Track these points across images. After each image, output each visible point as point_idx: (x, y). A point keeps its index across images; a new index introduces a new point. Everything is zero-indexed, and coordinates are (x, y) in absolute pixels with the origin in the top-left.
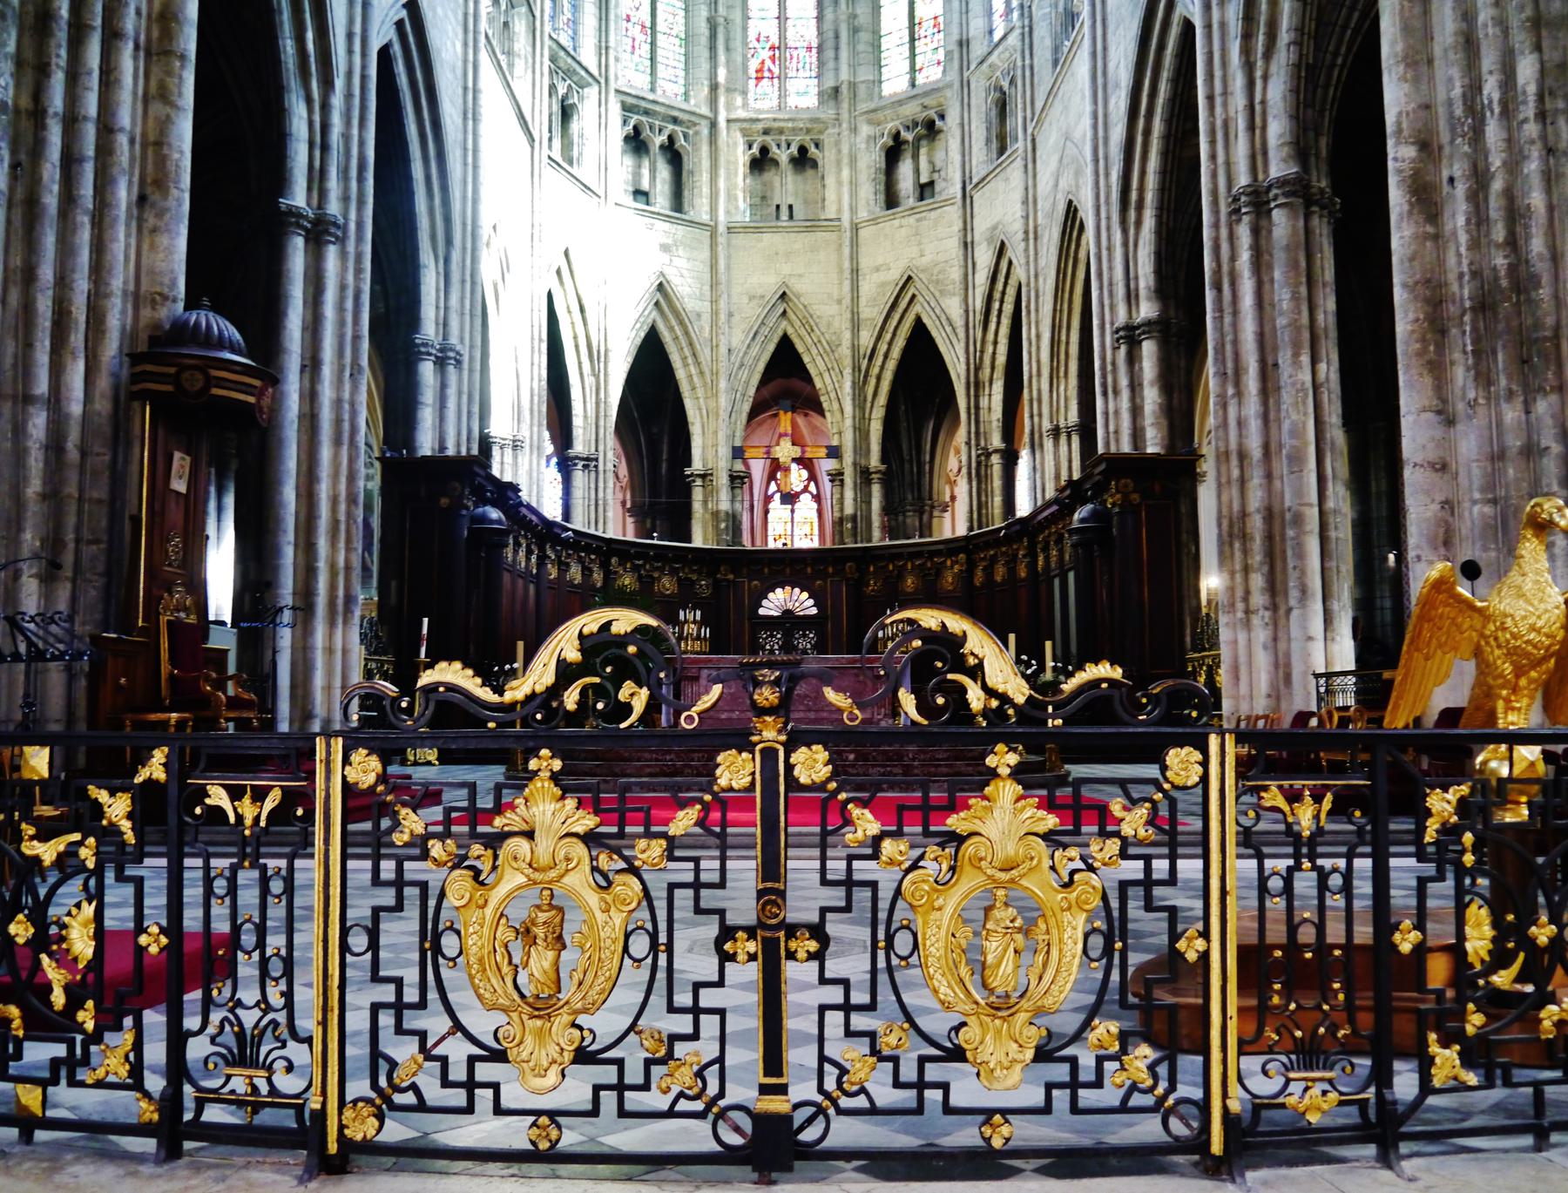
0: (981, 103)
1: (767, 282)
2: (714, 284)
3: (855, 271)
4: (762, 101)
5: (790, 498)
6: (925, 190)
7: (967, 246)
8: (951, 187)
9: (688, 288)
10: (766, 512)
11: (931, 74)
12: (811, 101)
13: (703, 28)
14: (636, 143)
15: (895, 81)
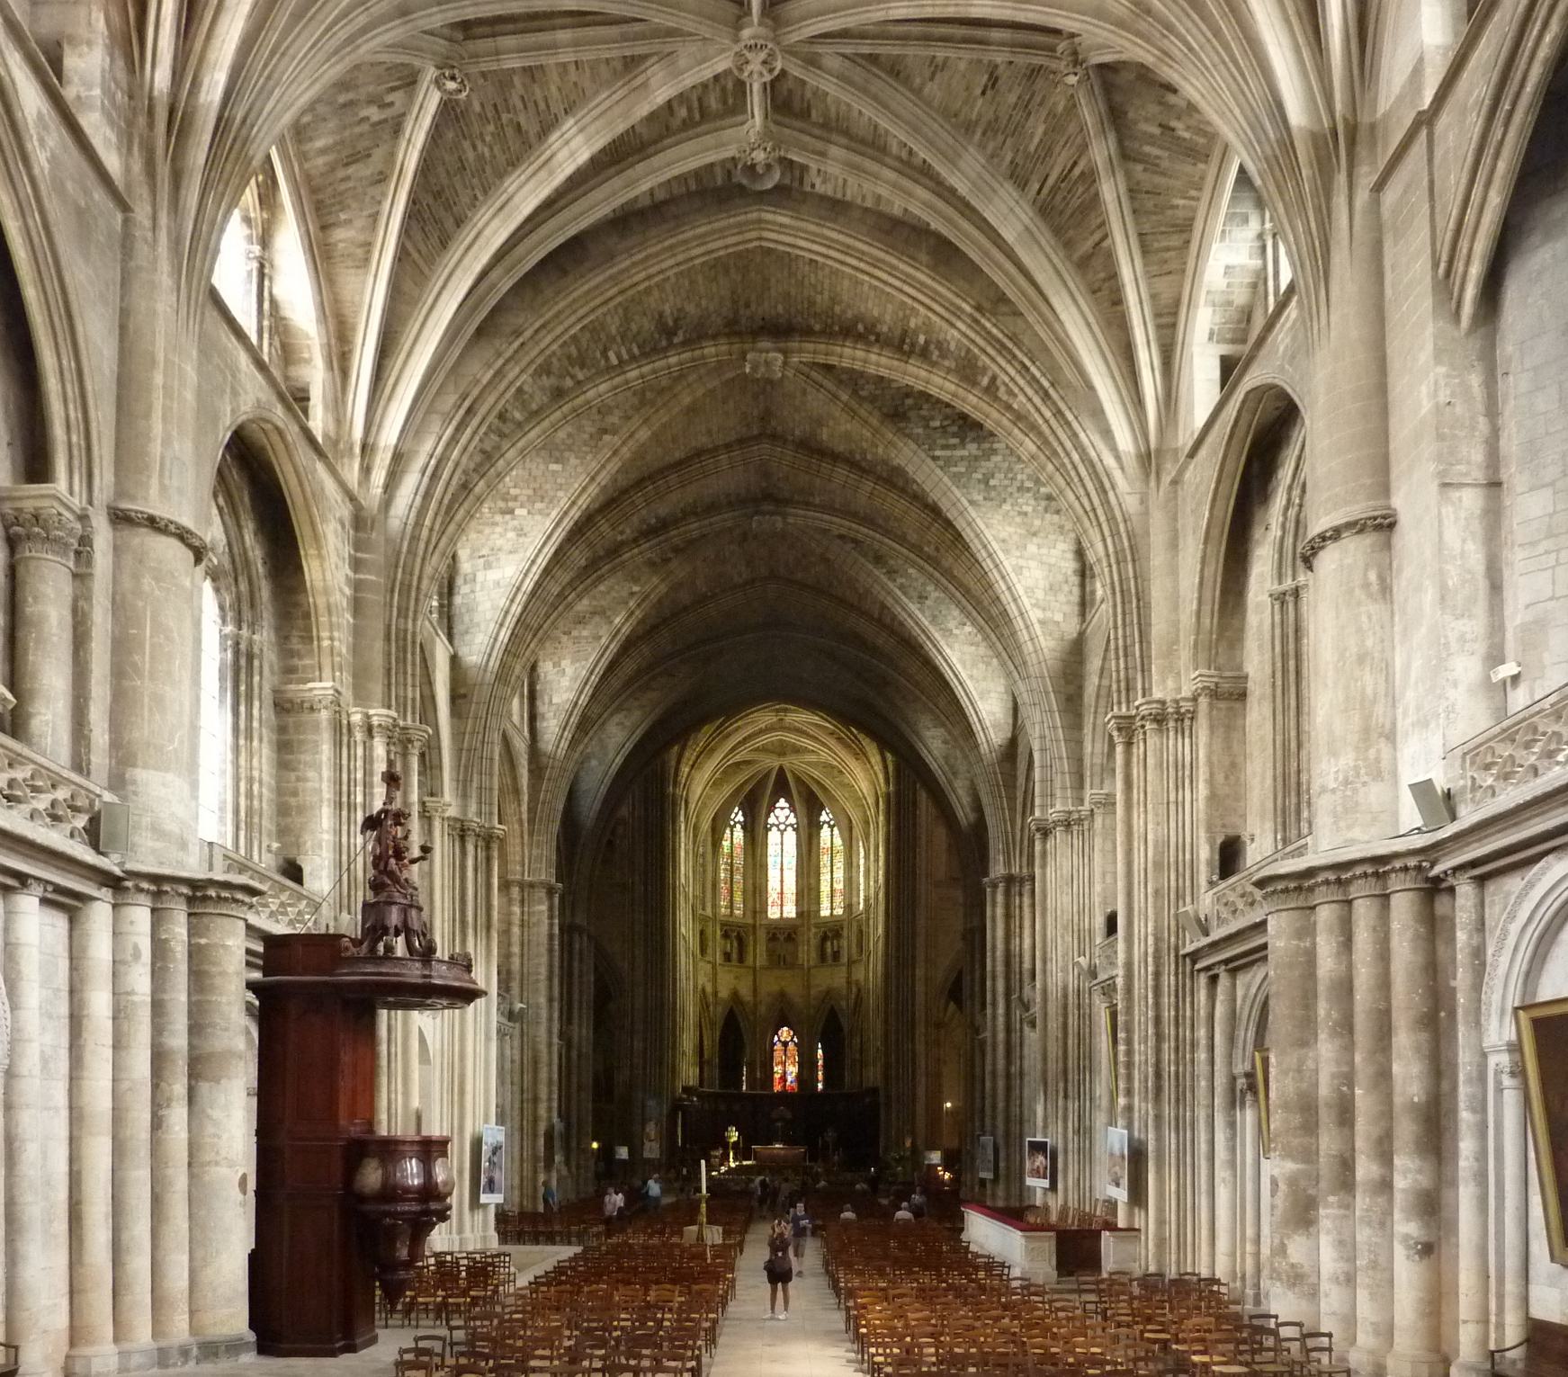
0: (855, 928)
1: (775, 988)
2: (755, 990)
3: (809, 987)
4: (773, 913)
5: (785, 1044)
6: (836, 955)
7: (849, 983)
8: (844, 959)
9: (745, 992)
10: (772, 1051)
11: (839, 911)
12: (793, 915)
13: (750, 887)
14: (726, 936)
15: (825, 912)
